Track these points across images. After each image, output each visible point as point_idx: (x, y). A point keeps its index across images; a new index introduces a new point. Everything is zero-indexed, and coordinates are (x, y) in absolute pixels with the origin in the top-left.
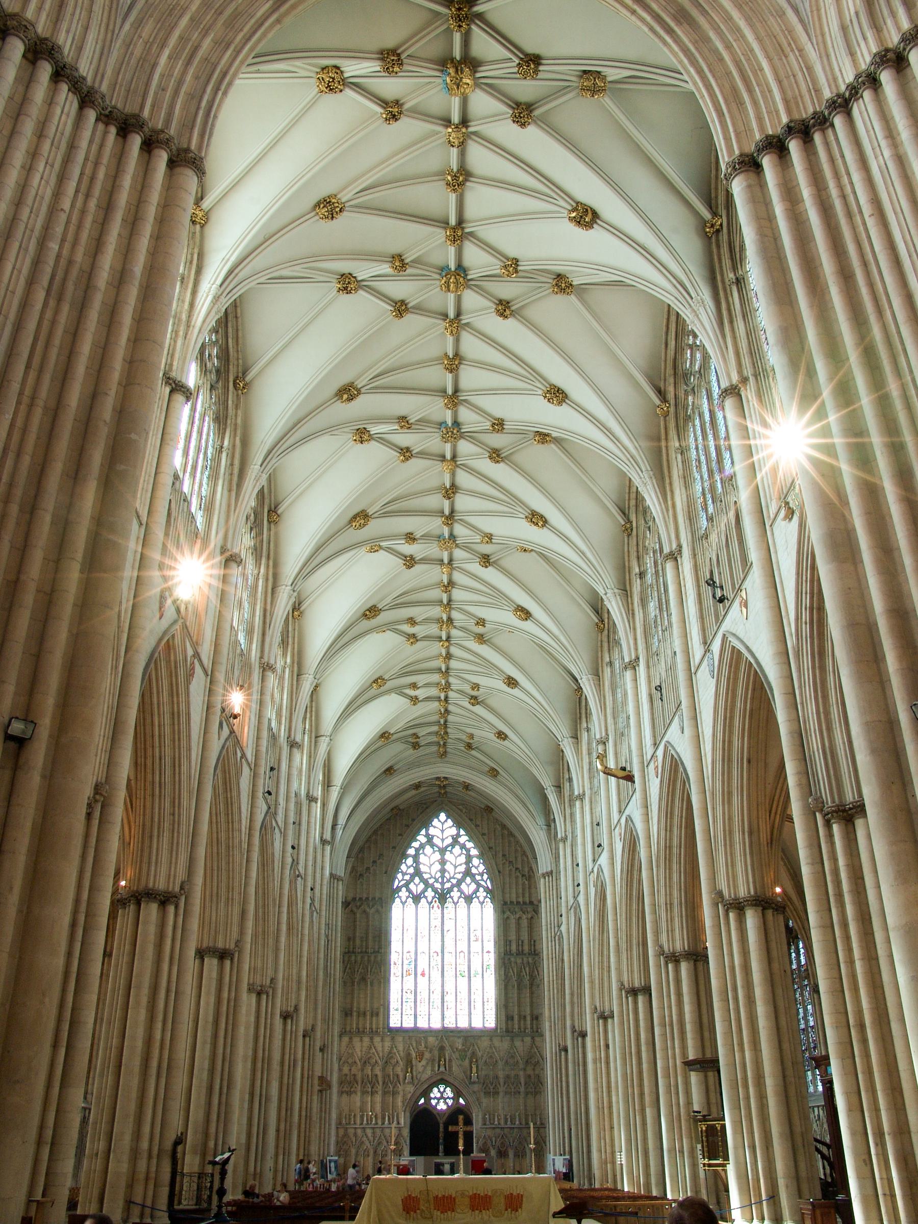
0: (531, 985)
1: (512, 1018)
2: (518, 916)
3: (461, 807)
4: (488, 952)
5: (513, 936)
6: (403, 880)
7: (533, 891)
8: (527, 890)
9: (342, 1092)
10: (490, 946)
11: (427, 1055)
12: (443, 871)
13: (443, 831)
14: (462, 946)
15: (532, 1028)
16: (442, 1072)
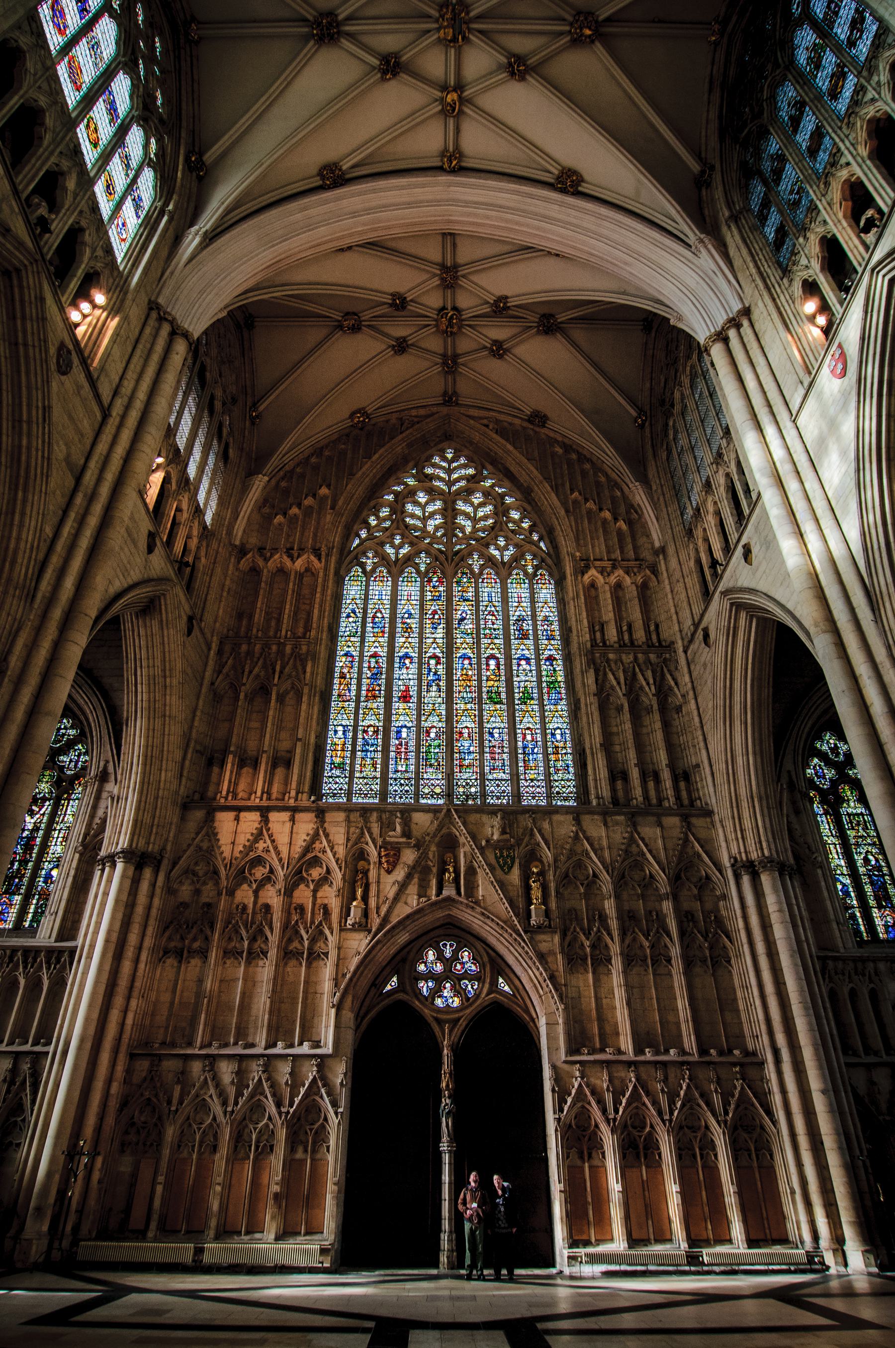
0: (663, 708)
1: (625, 776)
2: (613, 579)
3: (485, 422)
4: (551, 659)
5: (608, 614)
6: (371, 537)
7: (642, 540)
8: (629, 540)
9: (166, 952)
10: (552, 648)
11: (409, 856)
12: (450, 526)
13: (449, 472)
14: (493, 647)
15: (678, 798)
16: (449, 899)
